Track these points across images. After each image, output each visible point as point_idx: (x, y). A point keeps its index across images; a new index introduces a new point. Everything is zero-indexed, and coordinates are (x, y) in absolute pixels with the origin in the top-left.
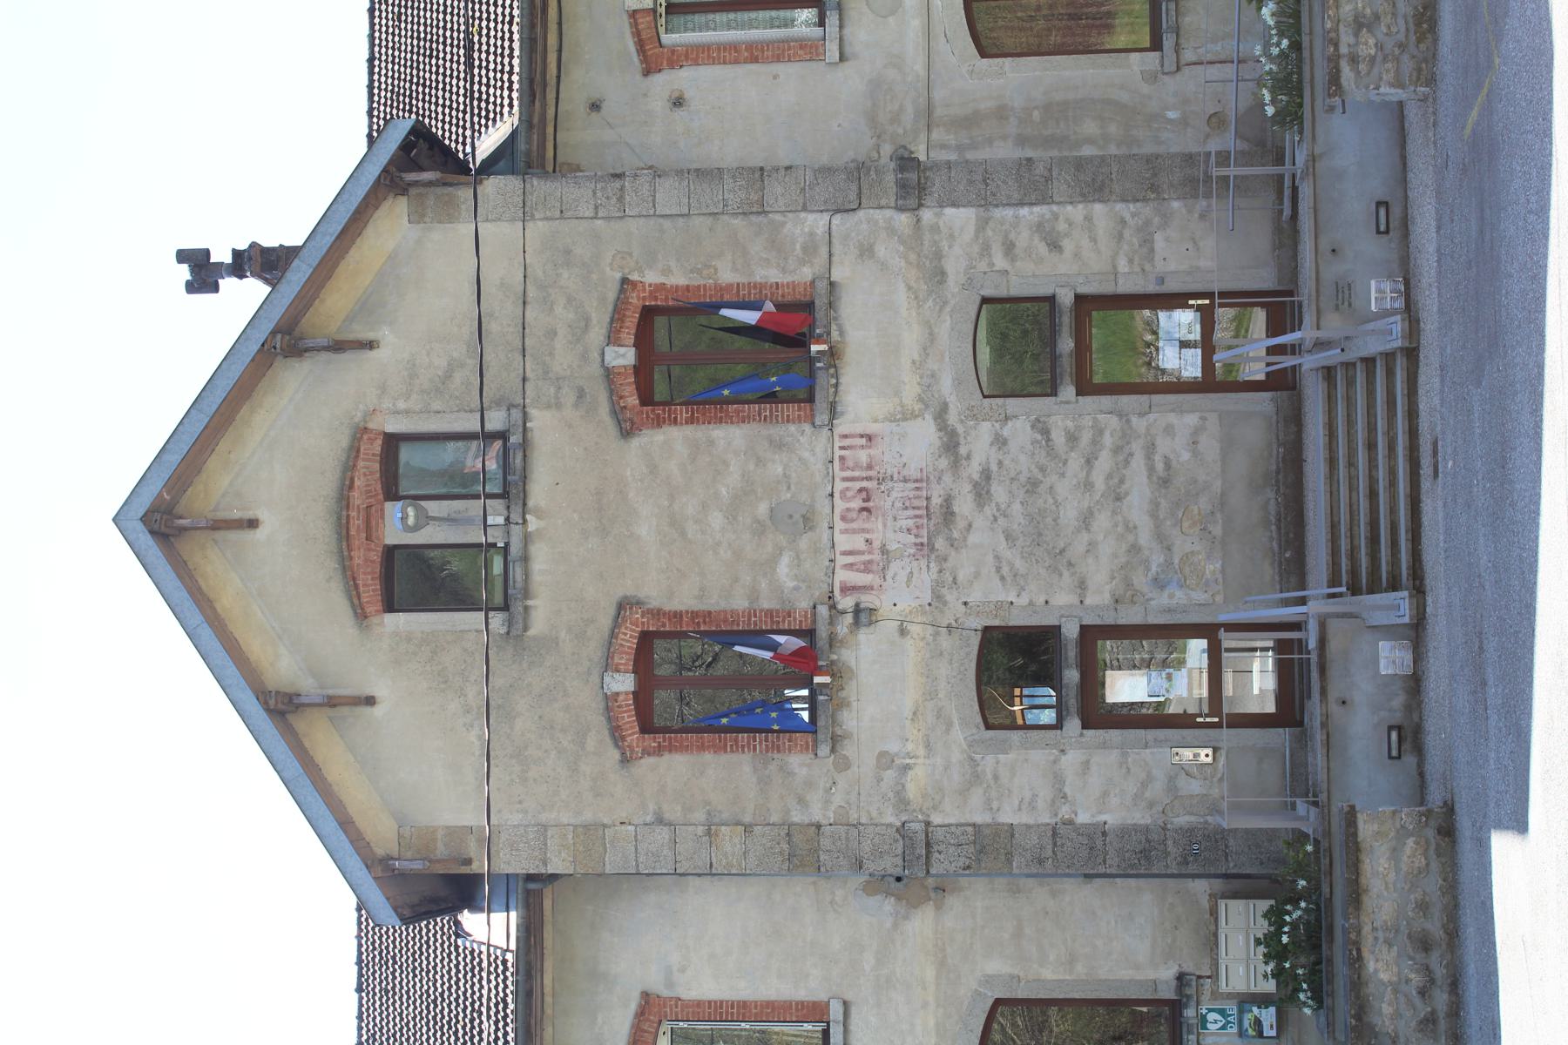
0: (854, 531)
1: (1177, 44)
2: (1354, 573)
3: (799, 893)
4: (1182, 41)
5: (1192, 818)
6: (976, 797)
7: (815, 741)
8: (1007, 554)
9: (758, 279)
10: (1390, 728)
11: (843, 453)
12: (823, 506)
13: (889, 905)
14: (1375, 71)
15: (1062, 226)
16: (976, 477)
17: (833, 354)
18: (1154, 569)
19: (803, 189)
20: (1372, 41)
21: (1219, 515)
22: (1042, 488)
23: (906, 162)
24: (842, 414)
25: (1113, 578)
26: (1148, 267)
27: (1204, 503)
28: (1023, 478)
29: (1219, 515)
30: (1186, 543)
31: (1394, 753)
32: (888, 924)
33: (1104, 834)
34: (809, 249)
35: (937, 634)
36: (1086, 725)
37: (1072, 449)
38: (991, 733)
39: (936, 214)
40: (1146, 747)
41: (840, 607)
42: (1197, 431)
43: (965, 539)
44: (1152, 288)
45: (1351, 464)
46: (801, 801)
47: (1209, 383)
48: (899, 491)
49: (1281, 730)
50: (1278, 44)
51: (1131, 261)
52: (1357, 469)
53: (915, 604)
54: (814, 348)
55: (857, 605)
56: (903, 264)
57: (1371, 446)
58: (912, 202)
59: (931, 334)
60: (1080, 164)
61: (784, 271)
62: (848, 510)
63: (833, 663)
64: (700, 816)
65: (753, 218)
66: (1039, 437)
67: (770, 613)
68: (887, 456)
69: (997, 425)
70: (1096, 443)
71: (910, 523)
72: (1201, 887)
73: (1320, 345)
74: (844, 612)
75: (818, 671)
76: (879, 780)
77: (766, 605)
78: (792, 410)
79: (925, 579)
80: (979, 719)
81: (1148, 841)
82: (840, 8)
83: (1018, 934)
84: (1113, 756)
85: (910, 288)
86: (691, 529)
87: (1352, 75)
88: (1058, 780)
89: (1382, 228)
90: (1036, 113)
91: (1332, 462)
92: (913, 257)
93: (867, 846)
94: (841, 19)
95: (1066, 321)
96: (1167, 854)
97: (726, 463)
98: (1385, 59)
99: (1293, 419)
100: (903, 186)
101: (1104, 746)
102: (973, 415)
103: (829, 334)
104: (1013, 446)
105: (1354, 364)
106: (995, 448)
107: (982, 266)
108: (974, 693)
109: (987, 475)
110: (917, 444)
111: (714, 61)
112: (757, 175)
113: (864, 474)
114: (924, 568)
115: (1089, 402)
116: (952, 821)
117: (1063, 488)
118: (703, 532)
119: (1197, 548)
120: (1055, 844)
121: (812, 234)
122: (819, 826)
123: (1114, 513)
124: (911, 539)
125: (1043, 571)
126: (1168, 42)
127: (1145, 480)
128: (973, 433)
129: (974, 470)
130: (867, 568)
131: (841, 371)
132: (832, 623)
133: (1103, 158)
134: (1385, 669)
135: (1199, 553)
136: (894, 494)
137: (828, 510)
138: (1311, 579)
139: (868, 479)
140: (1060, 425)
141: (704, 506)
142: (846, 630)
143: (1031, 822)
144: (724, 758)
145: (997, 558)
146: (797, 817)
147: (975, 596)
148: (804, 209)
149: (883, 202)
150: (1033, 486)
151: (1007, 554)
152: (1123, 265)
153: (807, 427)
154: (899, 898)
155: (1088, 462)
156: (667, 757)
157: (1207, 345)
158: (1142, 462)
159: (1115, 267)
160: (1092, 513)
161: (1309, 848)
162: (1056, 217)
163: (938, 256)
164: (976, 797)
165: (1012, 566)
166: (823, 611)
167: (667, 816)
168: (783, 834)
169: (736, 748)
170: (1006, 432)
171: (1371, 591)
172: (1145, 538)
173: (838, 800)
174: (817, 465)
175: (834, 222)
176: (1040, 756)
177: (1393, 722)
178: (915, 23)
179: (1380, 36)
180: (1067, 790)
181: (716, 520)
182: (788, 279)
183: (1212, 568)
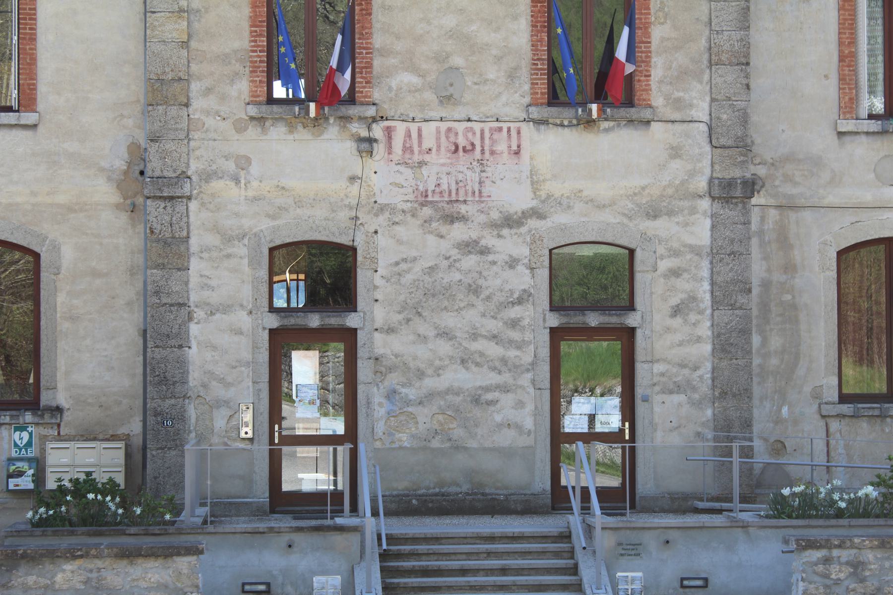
0: (438, 139)
1: (844, 416)
2: (399, 556)
3: (131, 88)
4: (847, 420)
5: (193, 421)
6: (212, 239)
7: (259, 103)
8: (417, 268)
9: (654, 60)
10: (268, 584)
11: (505, 130)
12: (460, 112)
13: (120, 164)
14: (817, 578)
15: (693, 317)
16: (483, 242)
17: (589, 123)
18: (404, 390)
19: (729, 99)
20: (842, 576)
21: (448, 445)
22: (472, 298)
23: (751, 186)
24: (538, 130)
25: (396, 356)
26: (657, 388)
27: (458, 433)
28: (481, 282)
29: (448, 445)
30: (425, 418)
31: (247, 588)
32: (104, 164)
34: (678, 104)
35: (351, 208)
37: (505, 323)
38: (266, 252)
39: (705, 213)
40: (254, 383)
41: (374, 126)
42: (519, 428)
43: (431, 232)
44: (639, 391)
45: (489, 554)
46: (208, 91)
47: (558, 437)
48: (472, 177)
49: (267, 494)
50: (841, 499)
51: (662, 374)
52: (485, 559)
53: (376, 190)
54: (594, 107)
55: (376, 141)
56: (664, 183)
57: (504, 571)
58: (716, 192)
59: (604, 206)
60: (745, 332)
61: (661, 82)
62: (457, 134)
63: (327, 119)
65: (706, 56)
66: (516, 296)
67: (369, 66)
68: (502, 168)
69: (526, 261)
71: (445, 187)
72: (135, 427)
73: (589, 530)
74: (369, 129)
76: (227, 158)
77: (377, 63)
78: (543, 87)
79: (398, 198)
80: (278, 242)
81: (174, 383)
82: (884, 132)
83: (95, 274)
84: (246, 355)
85: (643, 188)
87: (814, 559)
88: (226, 309)
89: (686, 583)
90: (789, 297)
91: (491, 539)
92: (670, 191)
93: (170, 146)
94: (874, 133)
95: (613, 320)
96: (164, 399)
97: (498, 29)
98: (826, 587)
99: (528, 507)
100: (729, 184)
101: (255, 347)
102: (535, 241)
103: (606, 119)
104: (508, 274)
105: (572, 558)
106: (507, 258)
107: (661, 250)
108: (300, 239)
109: (485, 251)
110: (510, 193)
111: (841, 23)
112: (743, 60)
113: (487, 148)
114: (406, 198)
115: (546, 337)
117: (472, 316)
119: (421, 426)
120: (172, 305)
121: (691, 106)
122: (187, 105)
123: (451, 358)
124: (431, 187)
125: (402, 298)
126: (846, 408)
127: (478, 384)
128: (520, 240)
129: (489, 240)
130: (408, 149)
131: (574, 129)
132: (361, 118)
133: (749, 352)
134: (318, 581)
135: (417, 428)
137: (457, 116)
138: (394, 520)
140: (526, 313)
141: (462, 11)
142: (354, 130)
143: (191, 285)
144: (246, 25)
145: (415, 259)
146: (195, 87)
147: (382, 240)
148: (713, 100)
149: (717, 167)
150: (474, 290)
151: (417, 268)
152: (659, 368)
153: (527, 100)
154: (126, 173)
155: (495, 337)
157: (590, 437)
158: (494, 382)
159: (658, 361)
161: (168, 517)
162: (701, 312)
163: (670, 213)
164: (212, 239)
165: (408, 271)
166: (371, 111)
168: (181, 74)
169: (254, 35)
170: (520, 268)
171: (383, 569)
172: (430, 383)
173: (210, 122)
175: (701, 125)
176: (246, 293)
177: (273, 587)
178: (867, 197)
179: (846, 583)
181: (450, 21)
183: (404, 439)
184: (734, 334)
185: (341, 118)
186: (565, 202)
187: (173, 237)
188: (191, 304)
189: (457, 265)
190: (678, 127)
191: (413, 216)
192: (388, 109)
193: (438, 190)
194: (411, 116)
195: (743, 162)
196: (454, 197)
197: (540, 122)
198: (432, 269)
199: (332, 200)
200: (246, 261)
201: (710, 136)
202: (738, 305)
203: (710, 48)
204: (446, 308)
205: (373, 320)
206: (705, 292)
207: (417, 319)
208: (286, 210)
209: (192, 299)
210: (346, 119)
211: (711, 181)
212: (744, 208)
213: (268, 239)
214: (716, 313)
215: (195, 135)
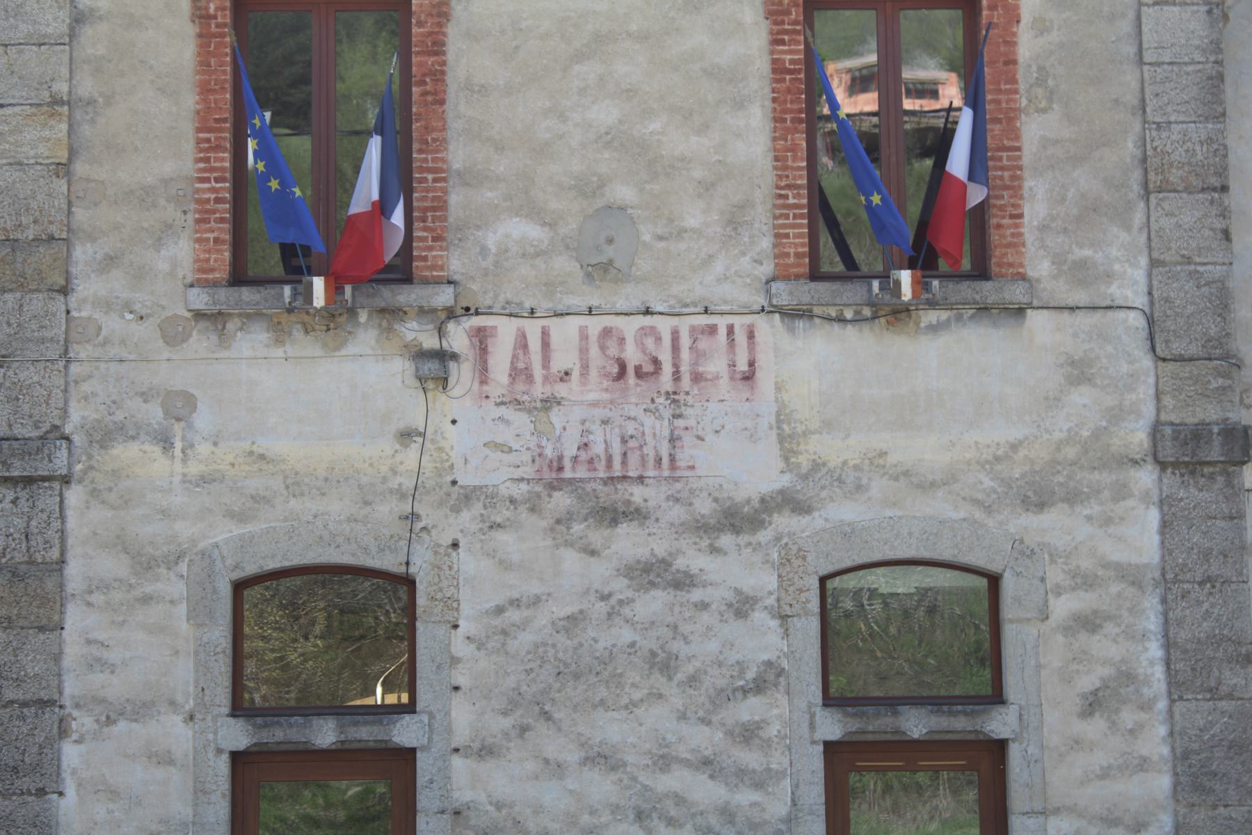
0: (583, 351)
6: (112, 566)
7: (215, 284)
8: (543, 618)
9: (1028, 183)
11: (722, 331)
12: (628, 297)
15: (1128, 717)
16: (680, 563)
17: (897, 314)
19: (1188, 260)
22: (659, 680)
24: (791, 330)
25: (499, 806)
28: (677, 646)
33: (41, 792)
34: (1081, 272)
35: (403, 496)
36: (237, 758)
37: (729, 733)
38: (226, 591)
41: (451, 326)
43: (569, 544)
46: (110, 262)
48: (656, 429)
53: (456, 458)
54: (905, 277)
55: (454, 356)
56: (1058, 435)
58: (1169, 451)
59: (933, 484)
61: (1043, 228)
62: (622, 340)
63: (352, 312)
64: (87, 86)
65: (1137, 175)
66: (750, 675)
67: (441, 206)
68: (717, 407)
69: (771, 601)
70: (742, 775)
71: (598, 449)
74: (441, 332)
75: (334, 289)
76: (145, 396)
77: (456, 199)
79: (499, 475)
80: (251, 569)
85: (1014, 447)
86: (589, 71)
88: (140, 710)
92: (1071, 452)
93: (29, 374)
95: (959, 724)
97: (704, 129)
100: (1196, 435)
101: (200, 791)
103: (932, 304)
104: (734, 628)
106: (730, 596)
107: (1055, 575)
108: (295, 561)
109: (683, 582)
110: (738, 463)
112: (1214, 181)
113: (685, 369)
114: (518, 473)
115: (815, 761)
116: (71, 523)
117: (658, 718)
118: (582, 91)
120: (25, 704)
121: (1109, 276)
122: (65, 291)
123: (615, 809)
124: (570, 450)
125: (511, 681)
129: (693, 559)
130: (519, 373)
131: (866, 327)
136: (648, 421)
137: (621, 305)
139: (677, 376)
141: (630, 93)
142: (410, 336)
143: (67, 662)
144: (187, 128)
145: (536, 601)
146: (82, 253)
147: (468, 562)
148: (1154, 263)
149: (1168, 401)
150: (664, 663)
151: (543, 618)
153: (767, 269)
155: (707, 762)
156: (191, 30)
159: (1057, 811)
160: (614, 769)
162: (1146, 706)
163: (1073, 498)
164: (112, 566)
165: (523, 625)
166: (444, 297)
167: (87, 31)
168: (53, 229)
169: (205, 149)
170: (759, 616)
173: (112, 324)
174: (704, 286)
175: (1132, 315)
176: (183, 676)
180: (122, 726)
181: (605, 114)
182: (1029, 237)
184: (1218, 753)
185: (383, 311)
186: (850, 477)
187: (31, 562)
188: (67, 701)
189: (626, 611)
190: (1084, 321)
191: (532, 510)
192: (478, 292)
193: (583, 456)
194: (527, 305)
195: (1224, 389)
196: (617, 470)
197: (794, 314)
198: (574, 621)
199: (364, 480)
200: (182, 609)
201: (1151, 337)
202: (1224, 689)
203: (1144, 160)
204: (602, 702)
205: (449, 731)
206: (1152, 663)
207: (542, 727)
208: (266, 500)
209: (68, 691)
210: (393, 313)
211: (1156, 431)
212: (1229, 484)
213: (229, 562)
214: (1179, 707)
215: (81, 351)
